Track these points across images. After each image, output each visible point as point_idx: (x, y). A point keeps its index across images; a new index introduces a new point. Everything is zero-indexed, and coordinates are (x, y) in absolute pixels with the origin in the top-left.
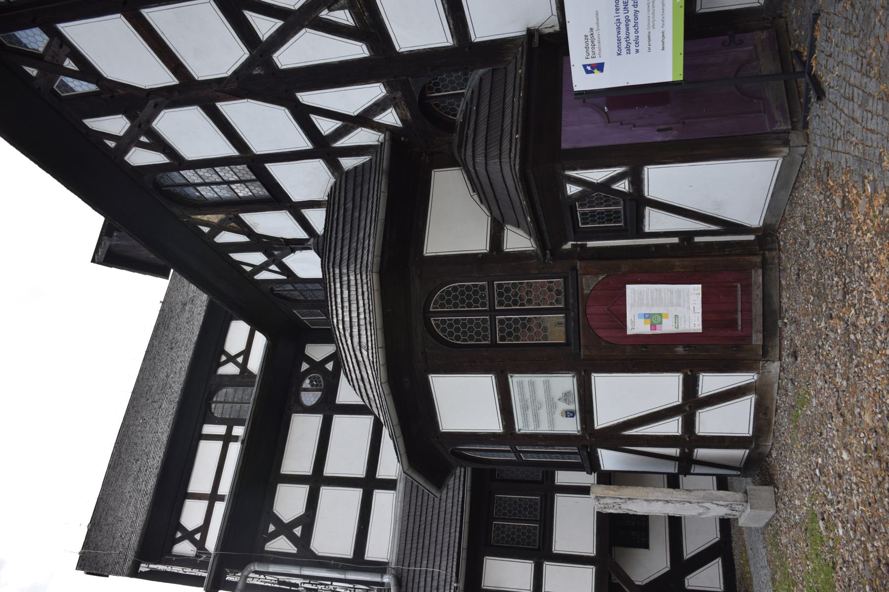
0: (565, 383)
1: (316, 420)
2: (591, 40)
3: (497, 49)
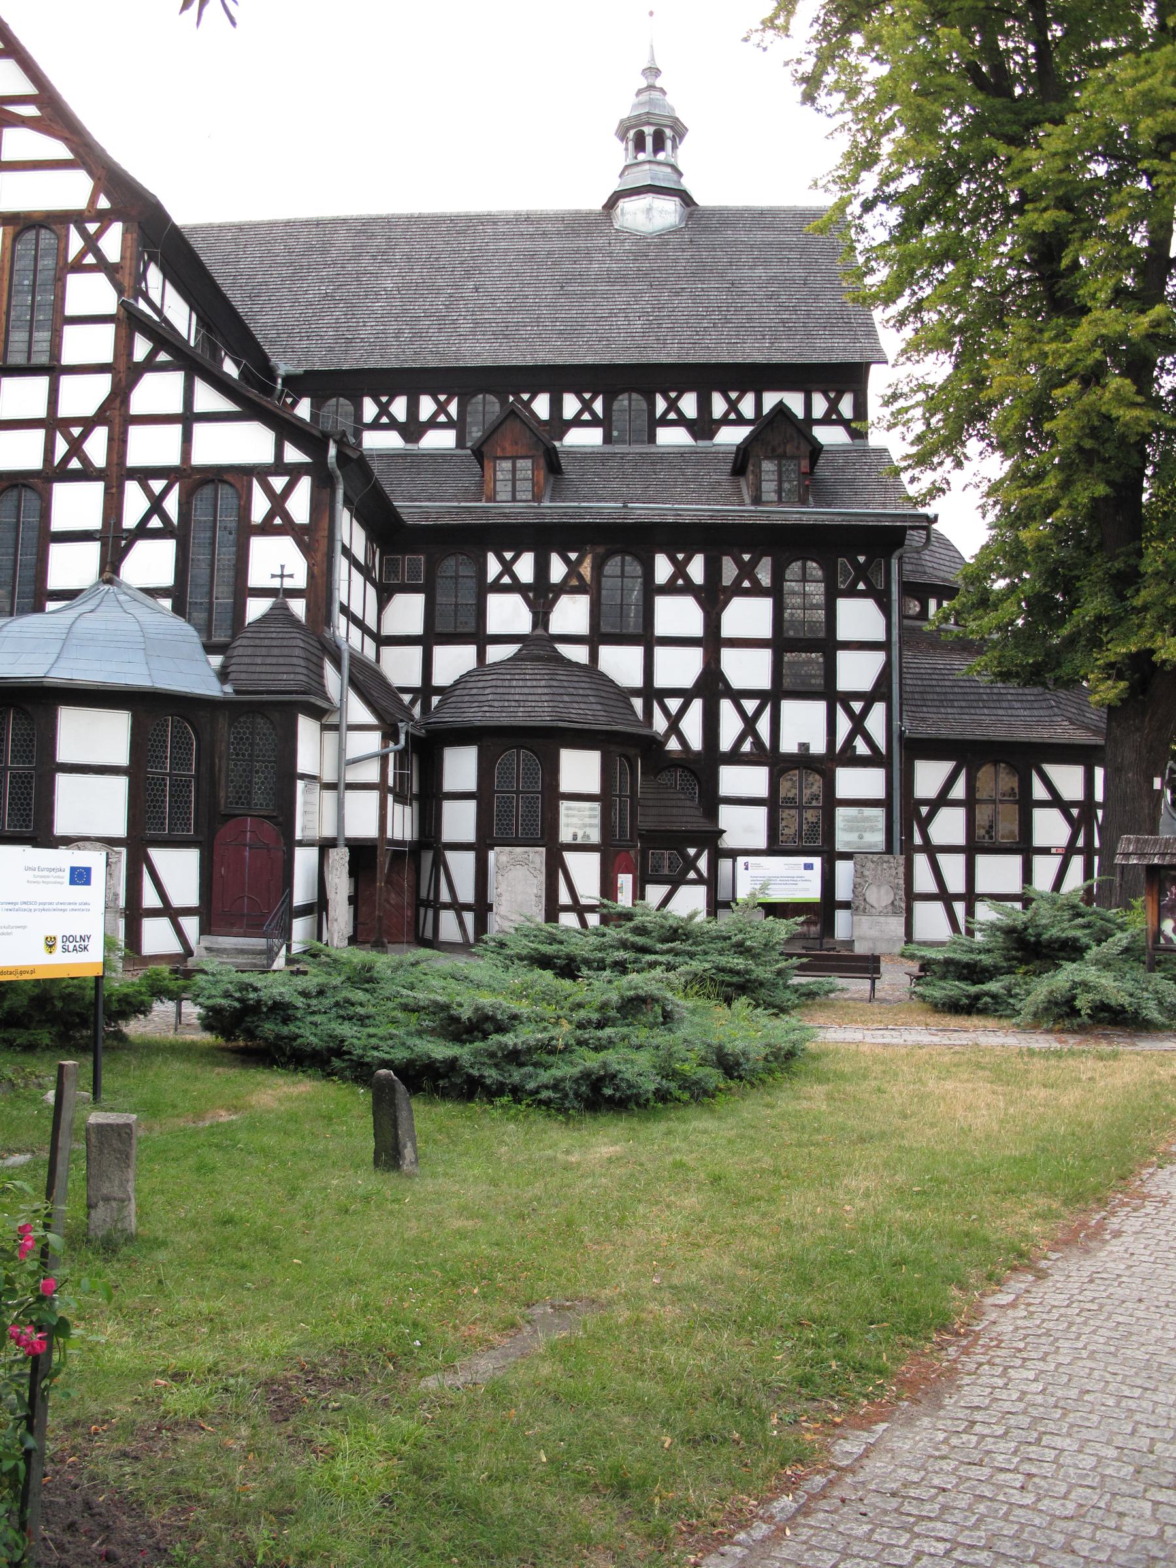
0: (595, 837)
2: (758, 866)
3: (713, 816)
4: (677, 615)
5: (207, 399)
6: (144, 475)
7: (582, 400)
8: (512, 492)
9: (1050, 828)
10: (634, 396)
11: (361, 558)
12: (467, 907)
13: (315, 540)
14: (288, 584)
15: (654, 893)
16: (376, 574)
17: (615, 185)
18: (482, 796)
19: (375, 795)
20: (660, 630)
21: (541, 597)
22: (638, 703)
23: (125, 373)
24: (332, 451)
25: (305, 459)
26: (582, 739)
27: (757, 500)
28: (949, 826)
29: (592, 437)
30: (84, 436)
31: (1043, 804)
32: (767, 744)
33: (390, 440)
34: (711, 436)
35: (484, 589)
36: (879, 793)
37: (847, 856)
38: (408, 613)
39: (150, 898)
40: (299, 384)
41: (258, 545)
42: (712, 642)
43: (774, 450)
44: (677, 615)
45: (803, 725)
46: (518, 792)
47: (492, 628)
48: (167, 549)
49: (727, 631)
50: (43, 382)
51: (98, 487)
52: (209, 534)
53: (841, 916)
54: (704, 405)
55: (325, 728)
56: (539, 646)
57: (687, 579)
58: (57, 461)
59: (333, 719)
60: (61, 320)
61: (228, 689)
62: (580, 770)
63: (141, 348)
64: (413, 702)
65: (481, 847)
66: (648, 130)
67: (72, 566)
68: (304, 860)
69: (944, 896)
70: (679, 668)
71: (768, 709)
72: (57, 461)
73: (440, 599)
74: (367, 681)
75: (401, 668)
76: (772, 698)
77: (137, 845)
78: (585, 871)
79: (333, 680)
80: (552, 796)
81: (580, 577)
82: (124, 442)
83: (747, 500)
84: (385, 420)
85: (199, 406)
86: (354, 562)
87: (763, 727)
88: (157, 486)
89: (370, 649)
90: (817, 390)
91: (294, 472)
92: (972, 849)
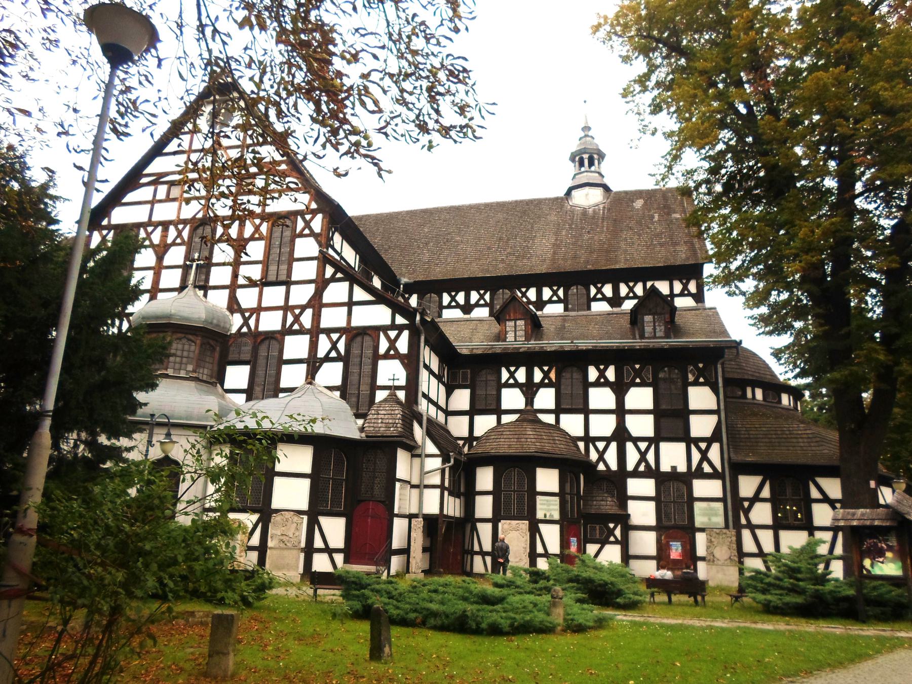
0: (557, 516)
3: (624, 506)
4: (602, 398)
5: (360, 294)
6: (328, 331)
7: (552, 290)
8: (515, 335)
9: (822, 515)
10: (579, 287)
11: (436, 372)
12: (487, 554)
13: (411, 362)
14: (397, 383)
15: (592, 549)
16: (445, 379)
17: (570, 183)
18: (496, 493)
19: (438, 491)
20: (592, 405)
21: (529, 390)
22: (581, 445)
23: (321, 284)
24: (418, 318)
25: (406, 322)
26: (548, 462)
27: (642, 336)
28: (762, 513)
29: (558, 309)
30: (301, 313)
31: (817, 501)
32: (653, 467)
33: (457, 314)
34: (620, 306)
35: (500, 386)
36: (719, 494)
37: (702, 530)
38: (462, 399)
39: (318, 543)
40: (410, 289)
41: (382, 363)
42: (621, 411)
43: (650, 310)
44: (602, 398)
45: (673, 456)
46: (514, 491)
47: (504, 406)
48: (340, 365)
49: (629, 405)
50: (283, 288)
51: (308, 337)
52: (359, 359)
53: (701, 565)
54: (616, 290)
55: (413, 456)
56: (529, 415)
57: (606, 378)
58: (287, 326)
59: (418, 452)
60: (292, 259)
61: (363, 435)
62: (547, 480)
63: (329, 271)
64: (464, 445)
65: (495, 521)
66: (586, 156)
67: (292, 376)
68: (399, 526)
69: (761, 554)
70: (603, 426)
71: (653, 447)
72: (287, 326)
73: (479, 392)
74: (437, 432)
75: (459, 427)
76: (654, 442)
77: (314, 513)
78: (551, 536)
79: (418, 432)
80: (533, 493)
81: (550, 379)
82: (320, 316)
83: (637, 336)
84: (453, 304)
85: (355, 299)
86: (431, 372)
87: (650, 457)
88: (335, 336)
89: (441, 417)
90: (676, 279)
91: (401, 328)
92: (777, 526)
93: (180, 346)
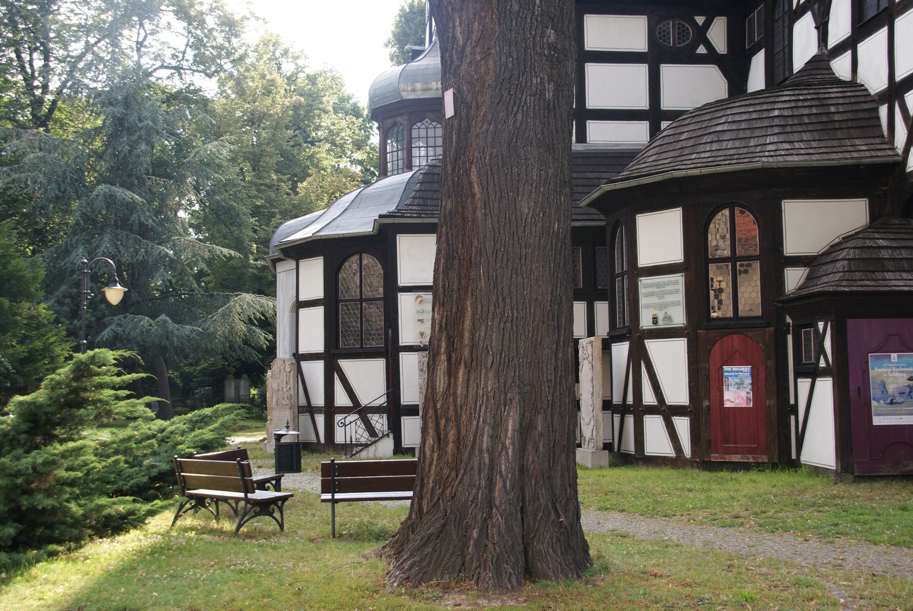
0: (679, 318)
1: (640, 44)
26: (656, 197)
93: (423, 133)
